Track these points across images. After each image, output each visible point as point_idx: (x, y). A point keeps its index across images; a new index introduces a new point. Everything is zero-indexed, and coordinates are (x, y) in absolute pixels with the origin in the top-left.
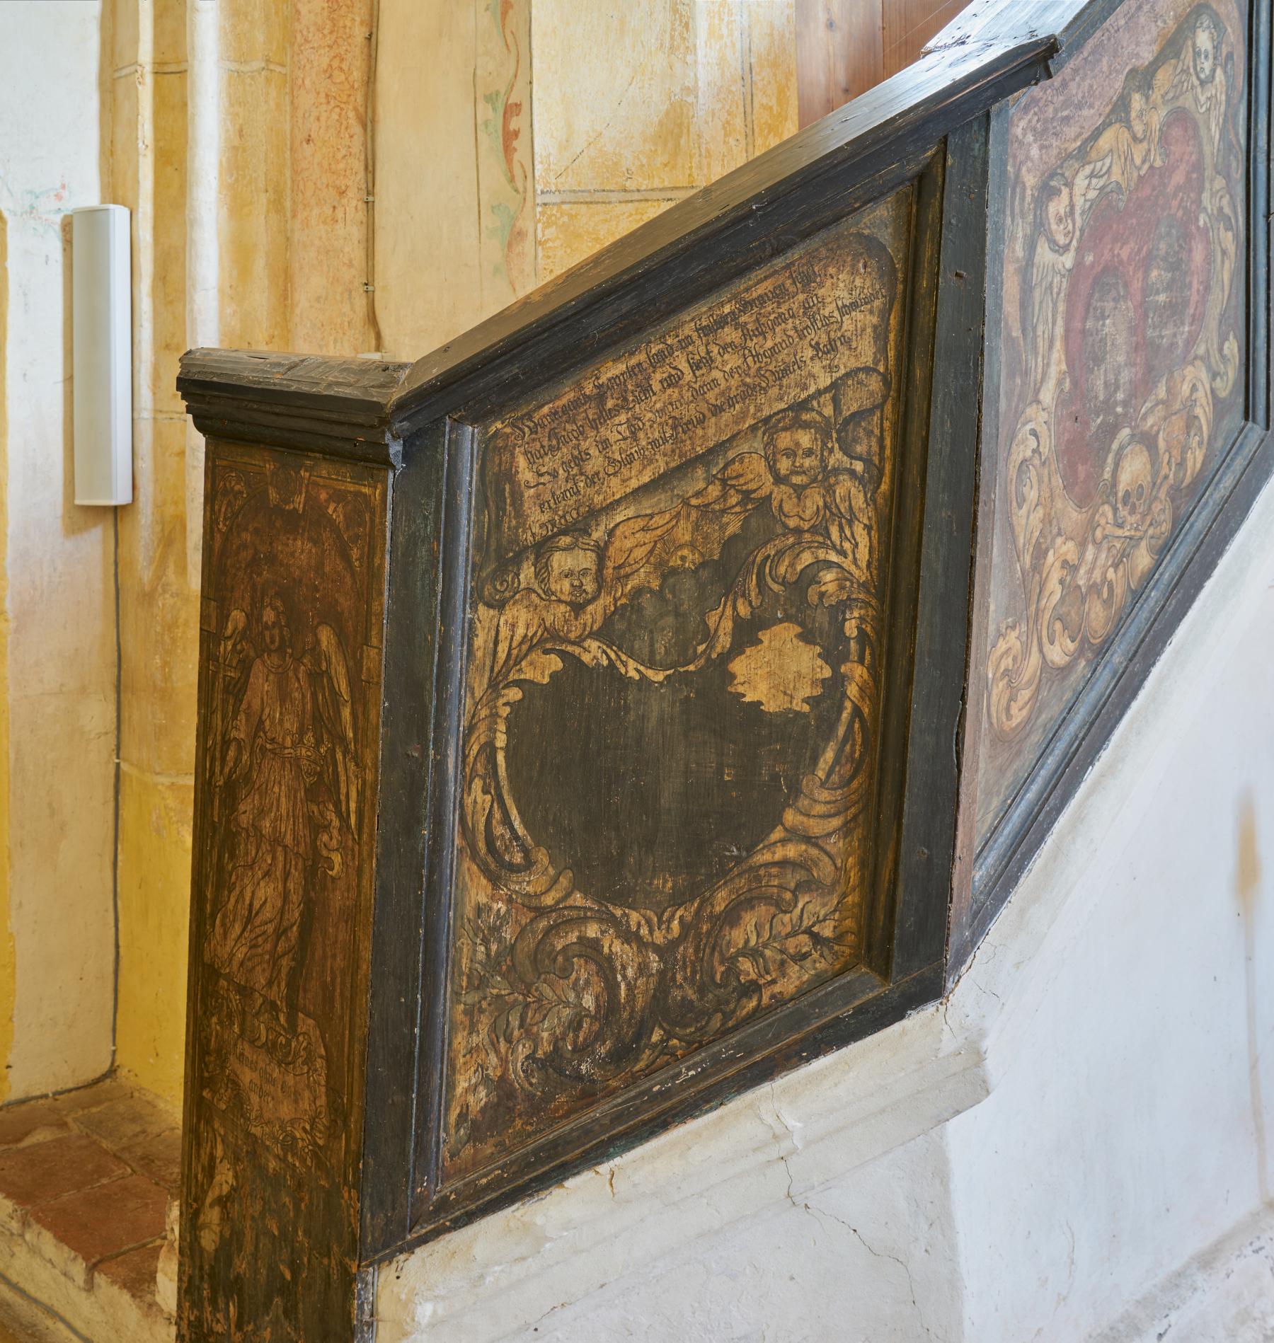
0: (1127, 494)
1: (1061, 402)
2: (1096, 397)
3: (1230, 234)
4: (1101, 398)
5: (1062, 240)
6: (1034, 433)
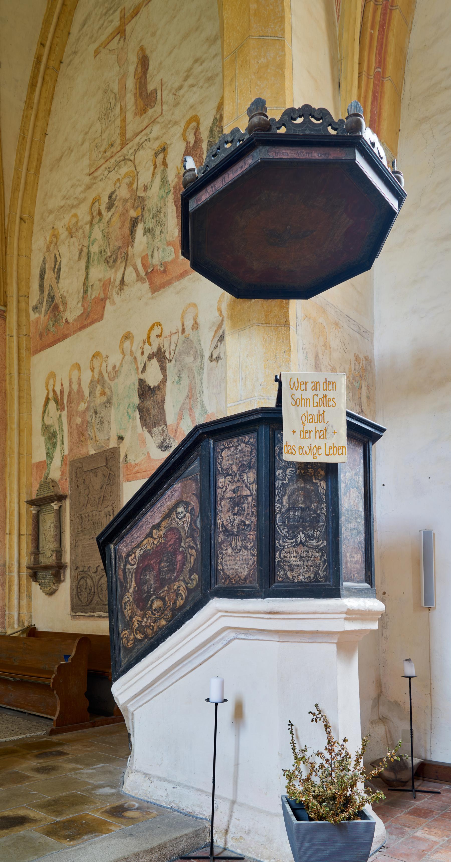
0: (155, 610)
3: (194, 550)
5: (133, 563)
6: (128, 597)
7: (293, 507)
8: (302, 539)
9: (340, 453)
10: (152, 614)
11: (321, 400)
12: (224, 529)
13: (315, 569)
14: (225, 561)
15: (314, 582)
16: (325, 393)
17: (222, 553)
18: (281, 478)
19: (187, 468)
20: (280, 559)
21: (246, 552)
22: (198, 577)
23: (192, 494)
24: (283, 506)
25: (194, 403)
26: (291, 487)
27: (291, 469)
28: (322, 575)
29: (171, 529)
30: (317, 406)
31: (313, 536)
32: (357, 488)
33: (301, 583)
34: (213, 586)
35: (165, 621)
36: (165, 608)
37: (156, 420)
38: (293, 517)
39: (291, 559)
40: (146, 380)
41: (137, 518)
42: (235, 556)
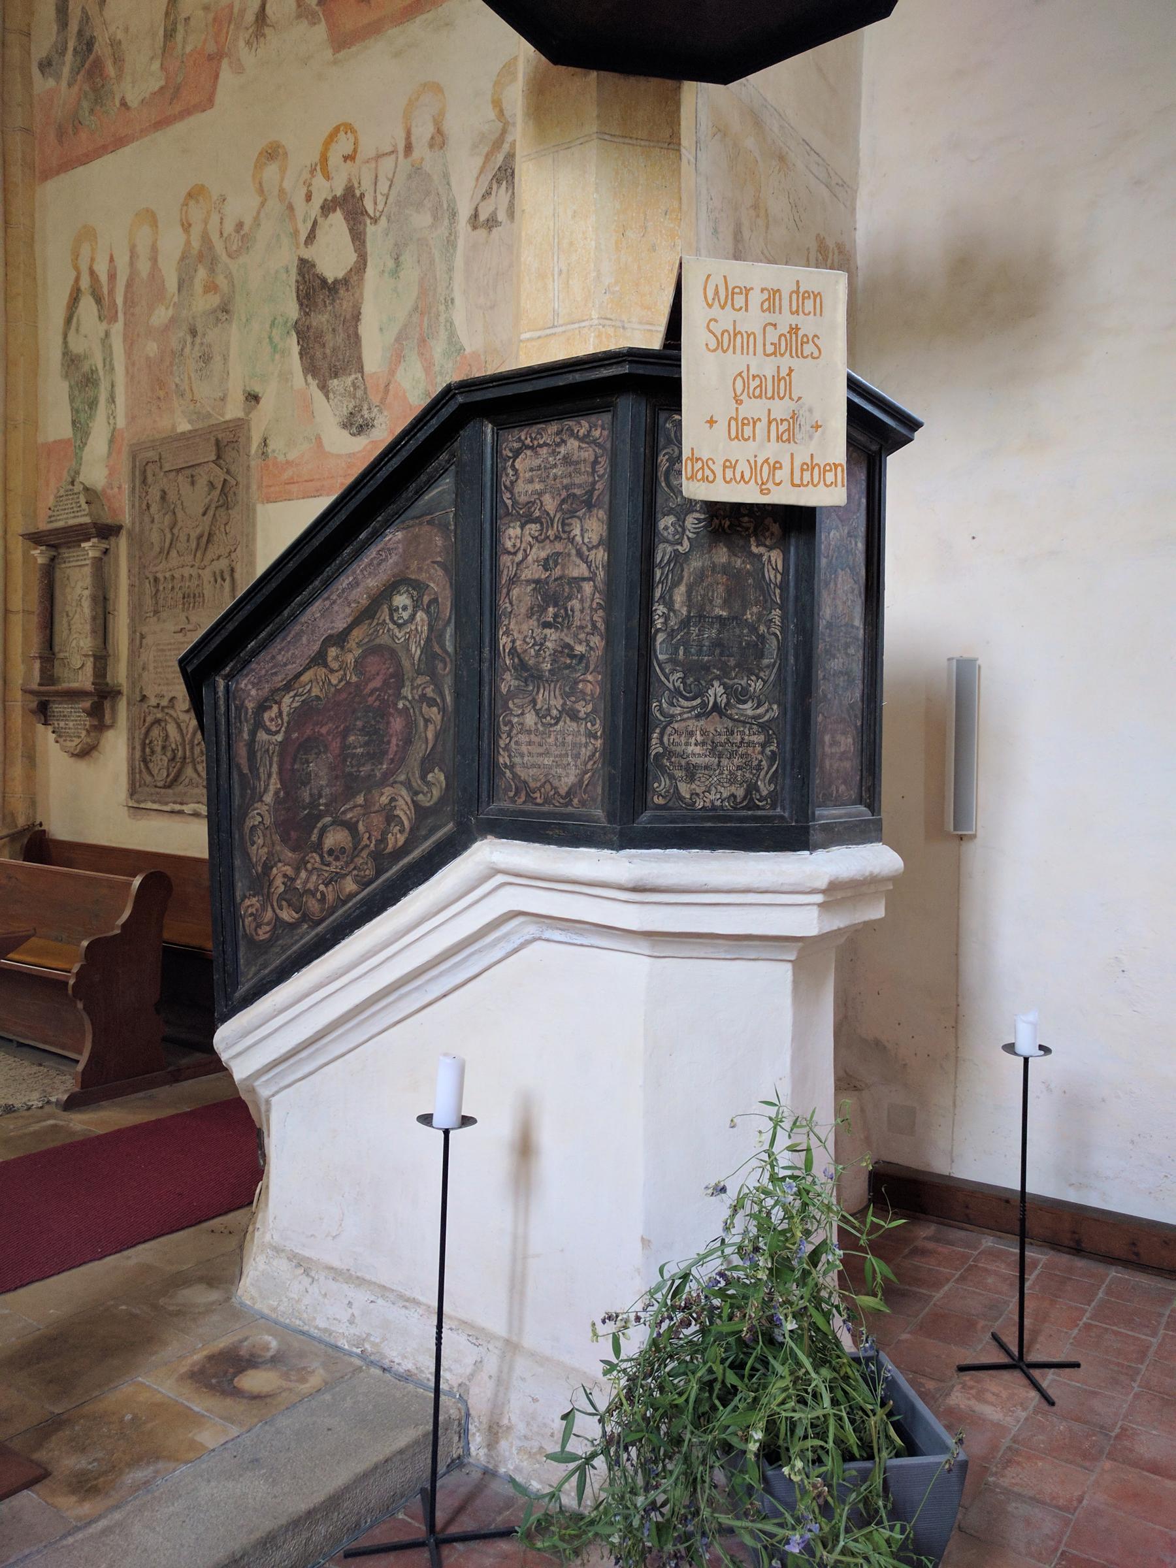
0: (331, 852)
1: (277, 800)
2: (304, 801)
3: (435, 709)
4: (307, 801)
5: (274, 729)
6: (258, 814)
7: (699, 616)
8: (719, 700)
9: (828, 482)
10: (323, 863)
11: (783, 338)
12: (516, 660)
13: (747, 775)
14: (517, 743)
15: (743, 808)
16: (794, 320)
17: (510, 722)
18: (670, 537)
19: (420, 493)
20: (661, 750)
21: (574, 725)
22: (446, 778)
23: (433, 562)
24: (674, 612)
26: (696, 563)
27: (697, 515)
28: (765, 793)
29: (373, 649)
30: (774, 353)
31: (745, 691)
32: (852, 569)
33: (712, 812)
34: (484, 804)
35: (356, 882)
36: (355, 849)
37: (339, 360)
38: (699, 641)
39: (690, 749)
40: (317, 262)
41: (286, 613)
42: (544, 733)
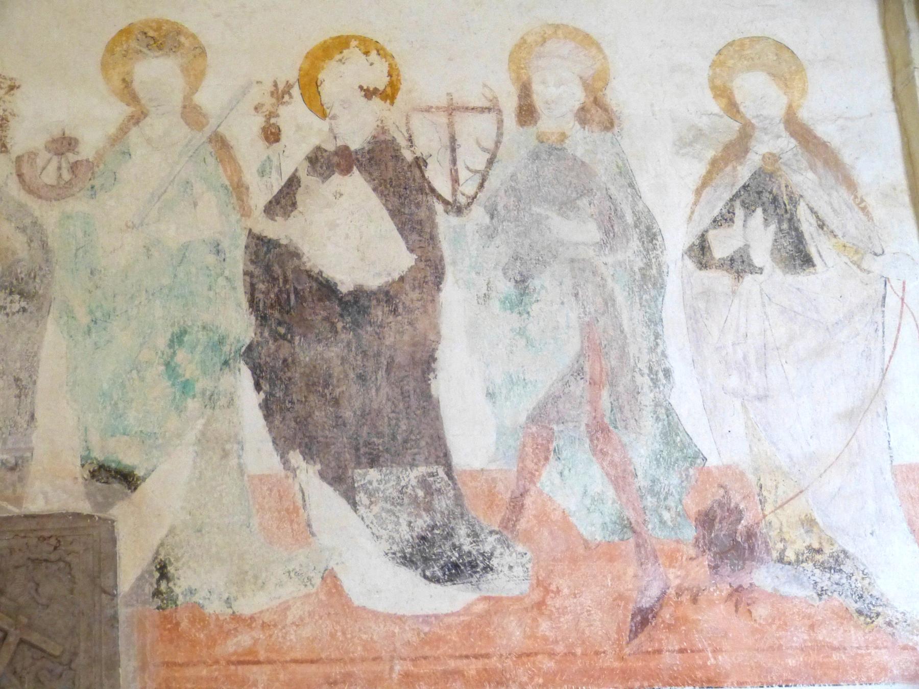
25: (616, 408)
